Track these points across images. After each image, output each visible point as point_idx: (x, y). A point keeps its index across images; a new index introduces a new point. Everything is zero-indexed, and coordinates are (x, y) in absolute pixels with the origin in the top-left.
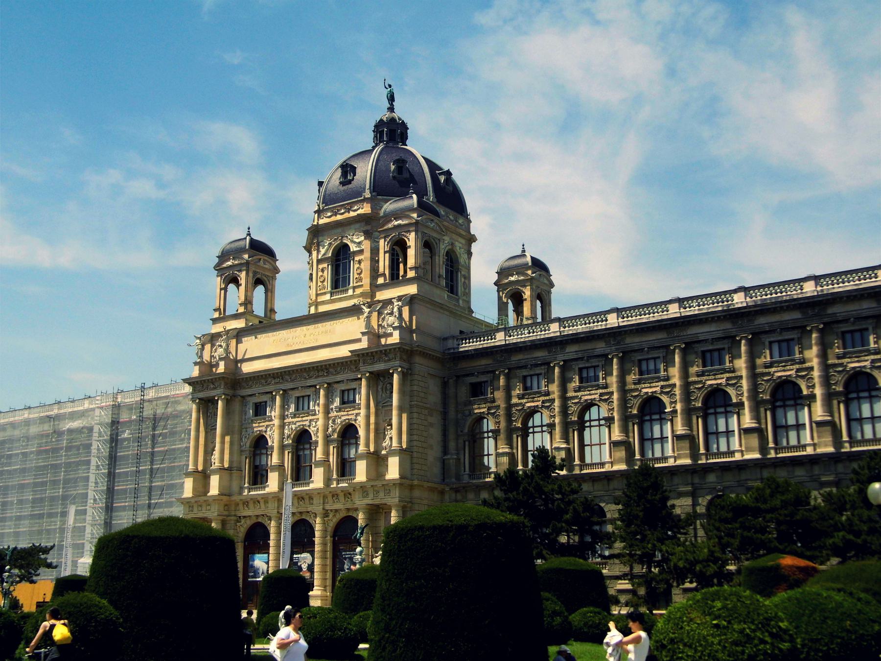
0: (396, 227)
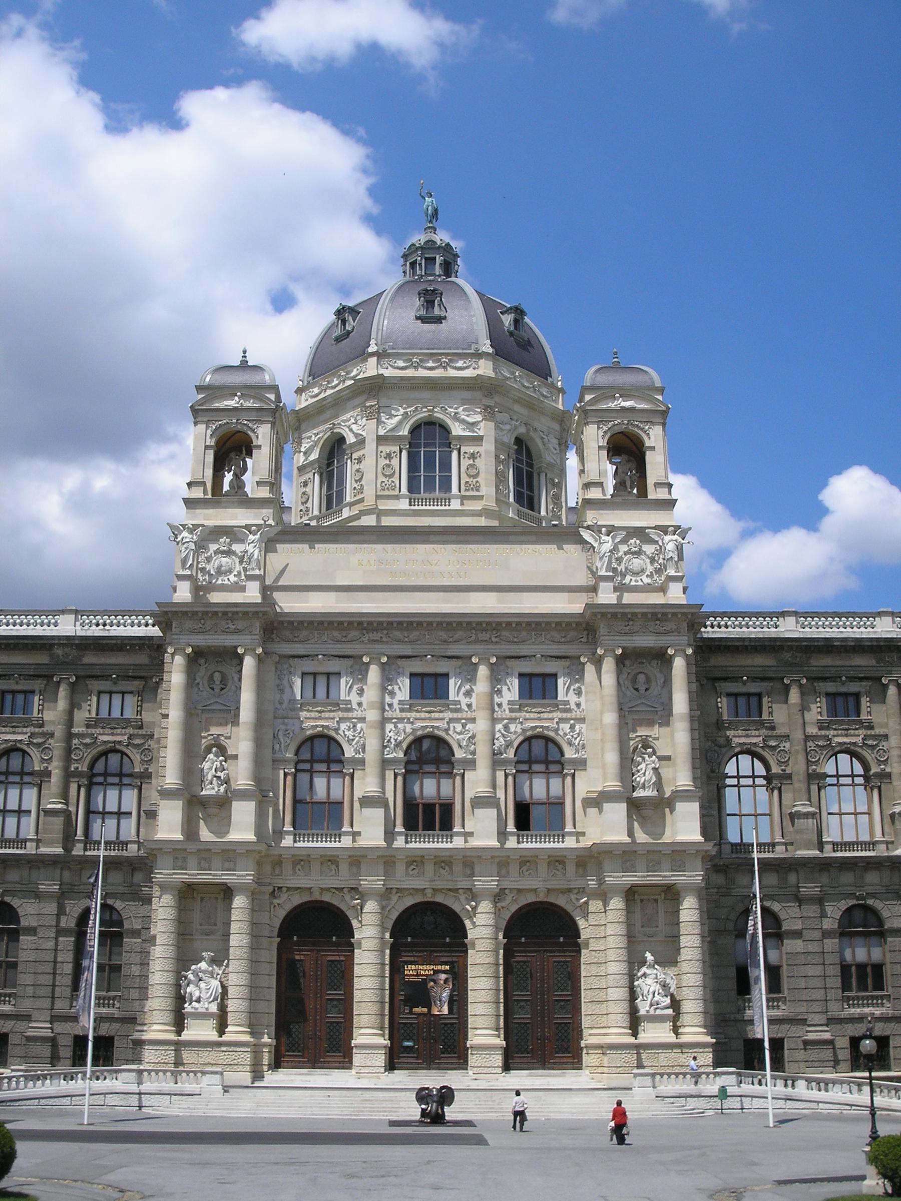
0: (623, 409)
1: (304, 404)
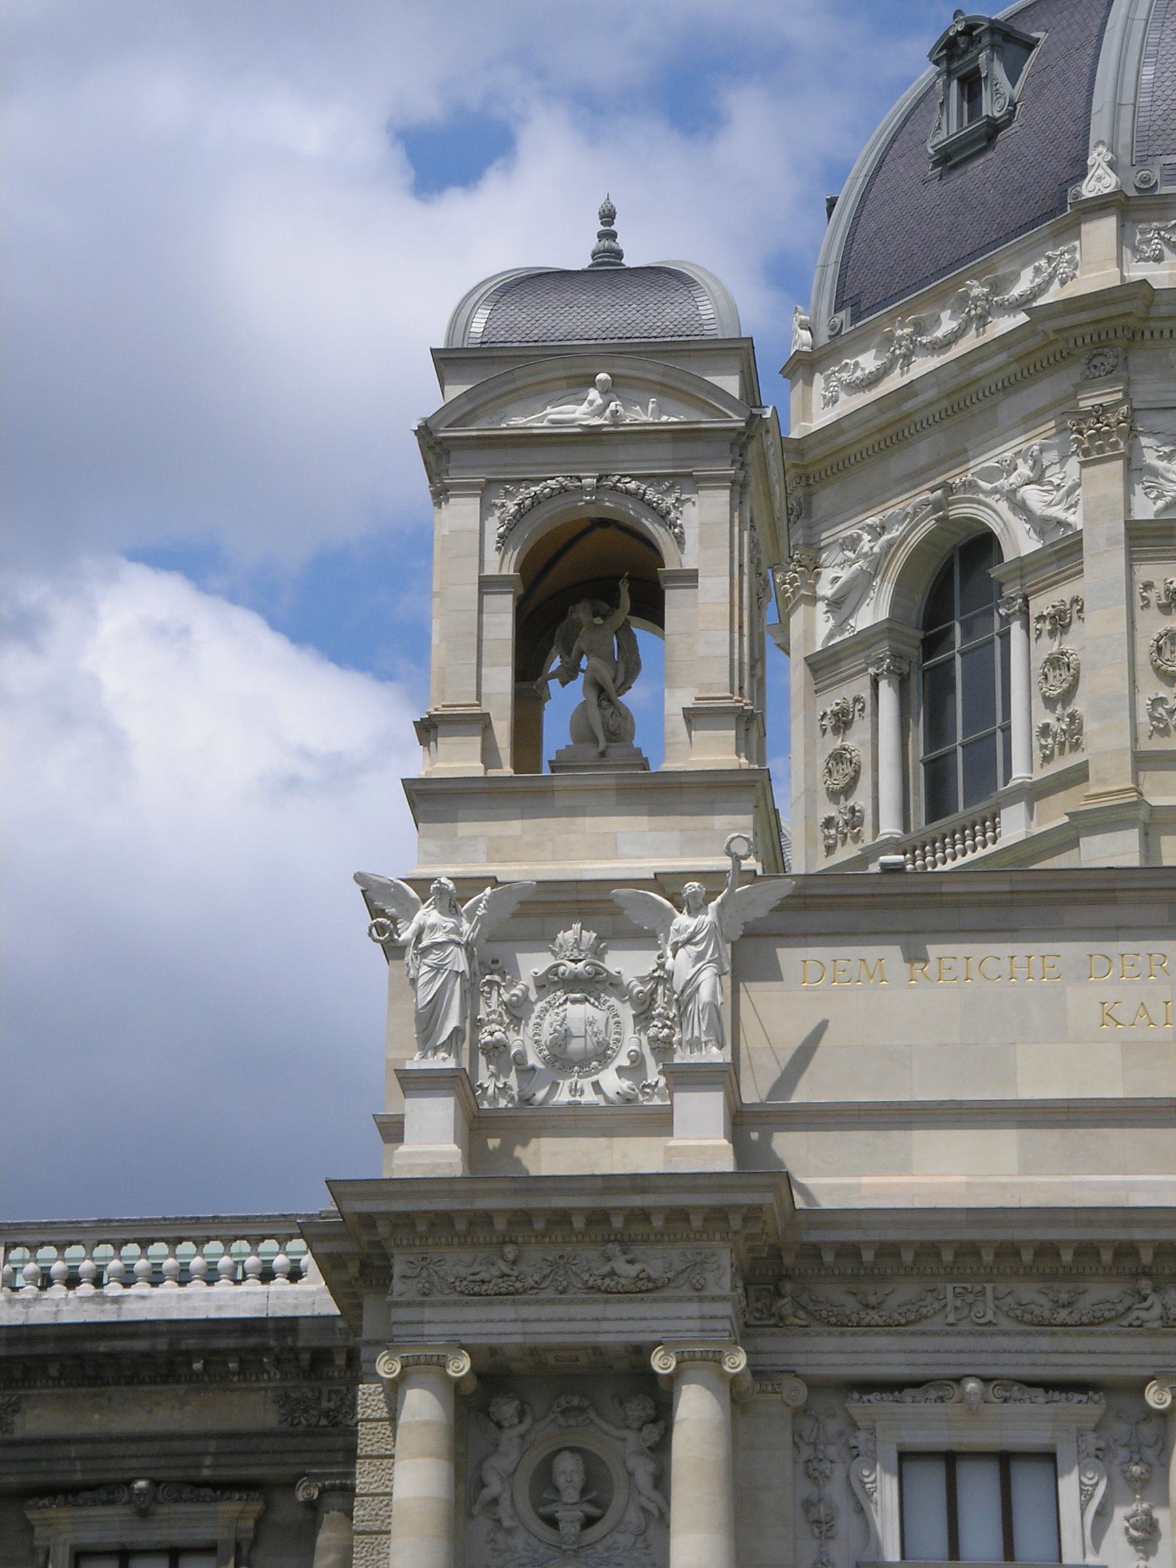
1: (821, 418)
